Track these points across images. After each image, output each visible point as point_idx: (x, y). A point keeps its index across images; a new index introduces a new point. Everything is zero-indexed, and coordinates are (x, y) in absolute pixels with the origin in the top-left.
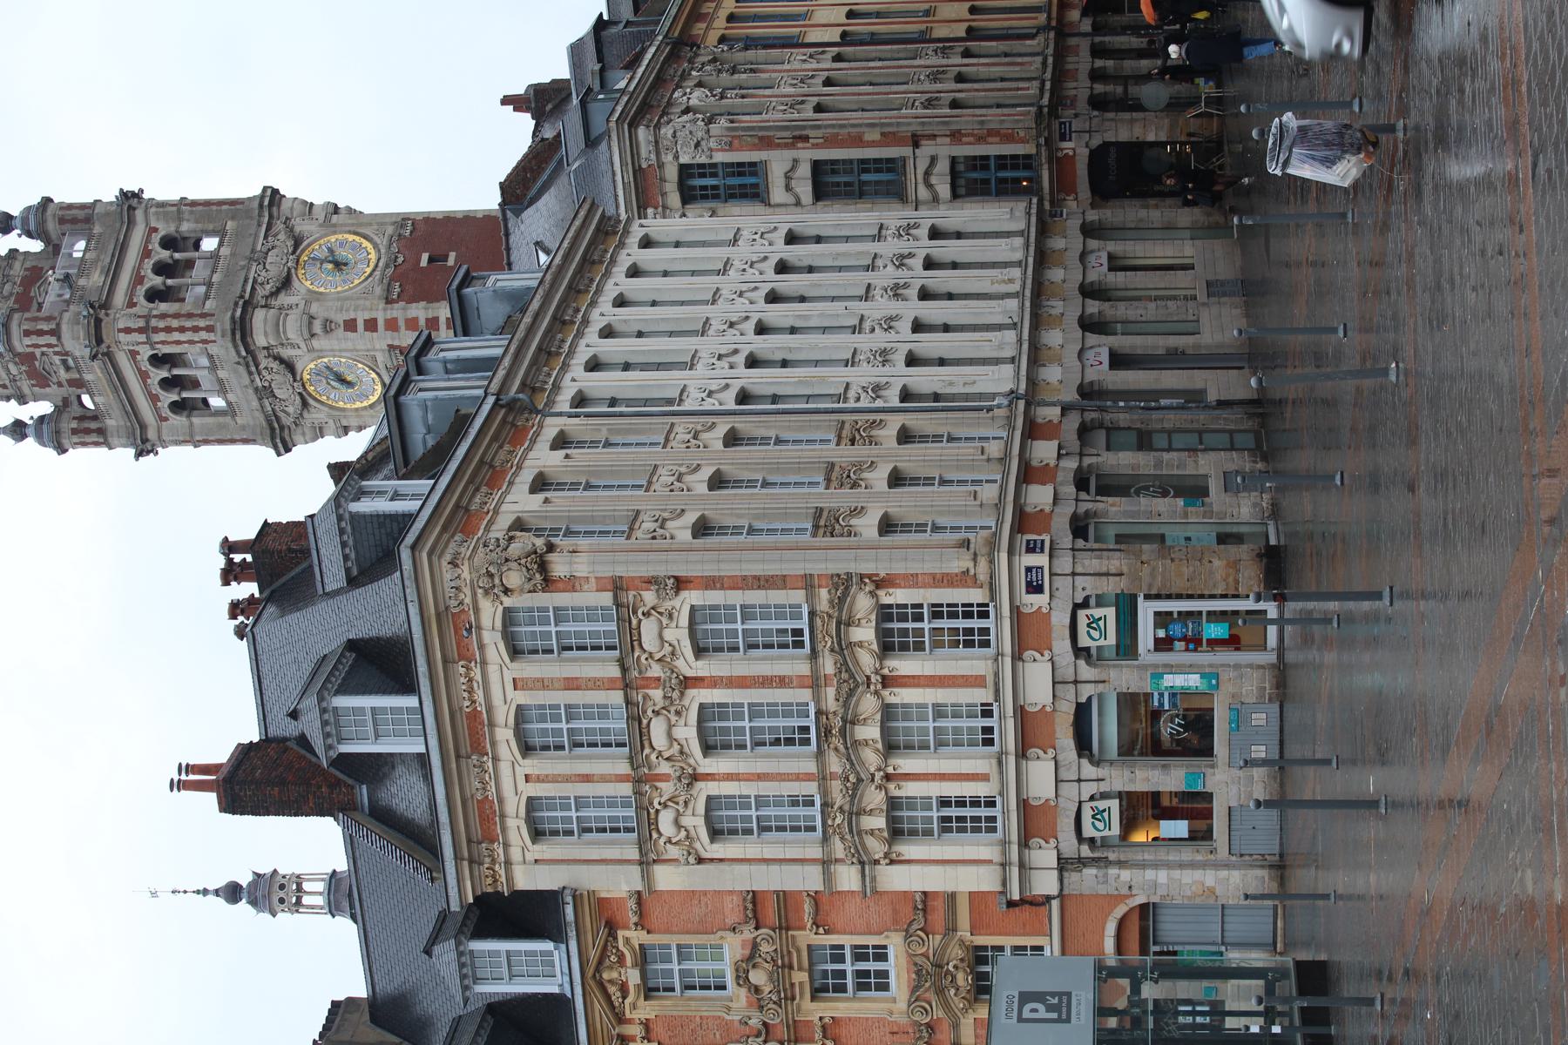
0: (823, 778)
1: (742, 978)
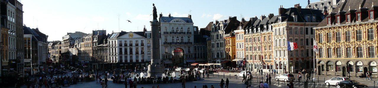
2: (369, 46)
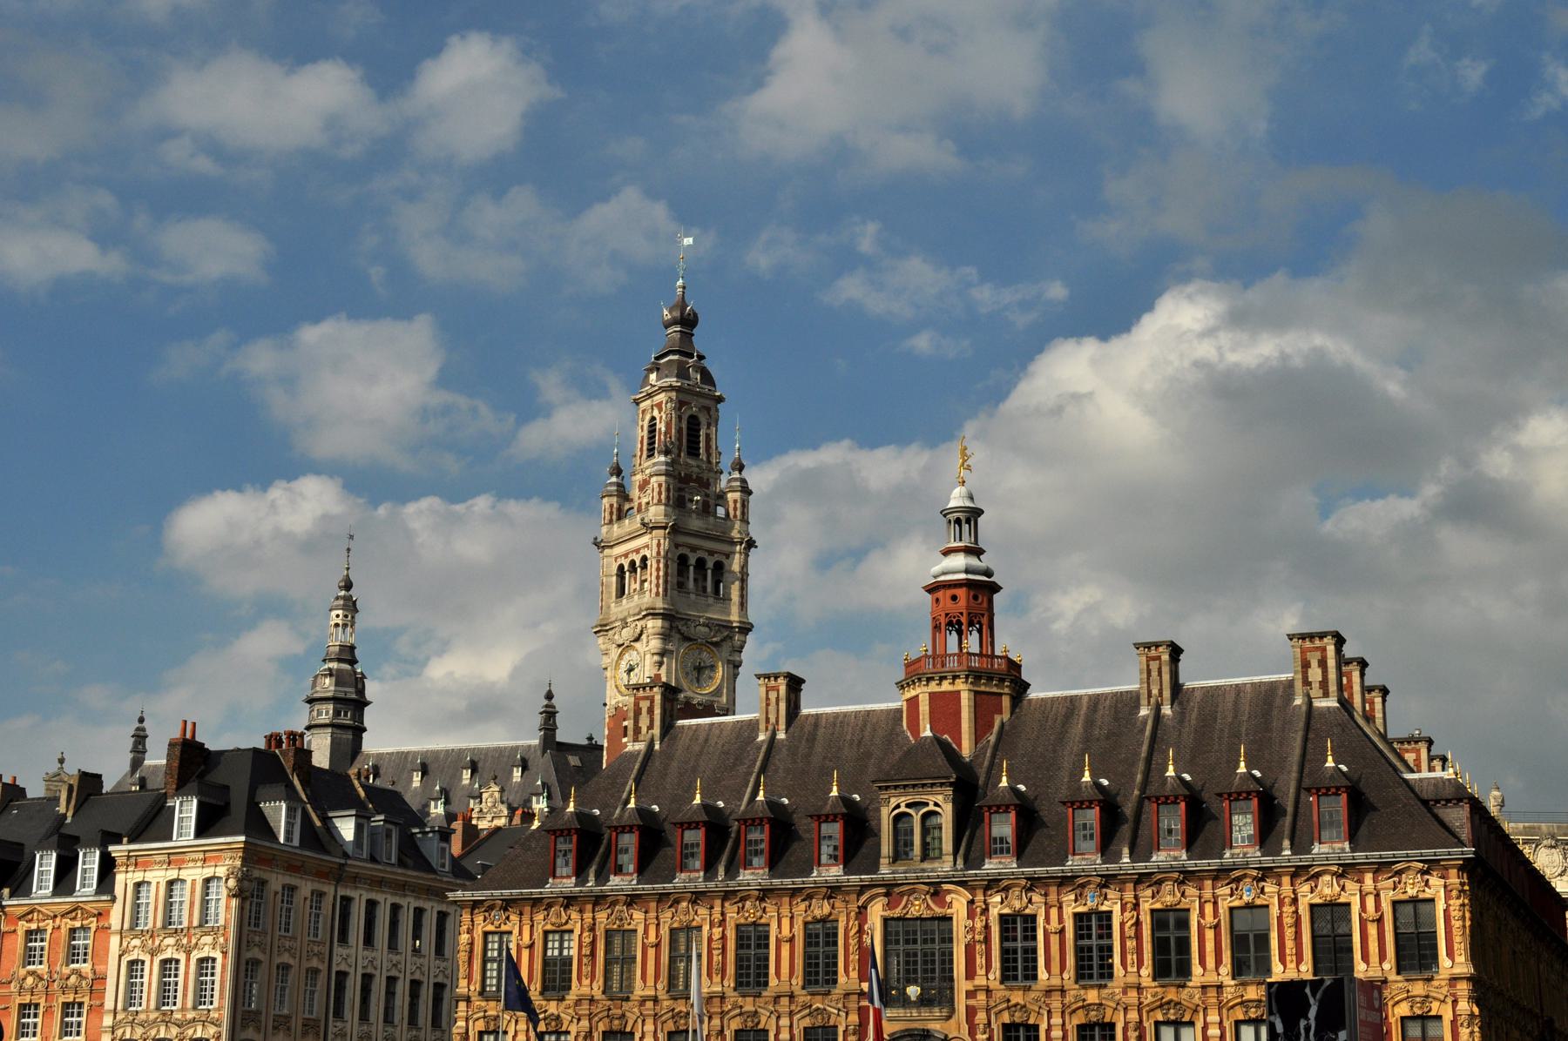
0: (147, 1011)
2: (807, 1022)
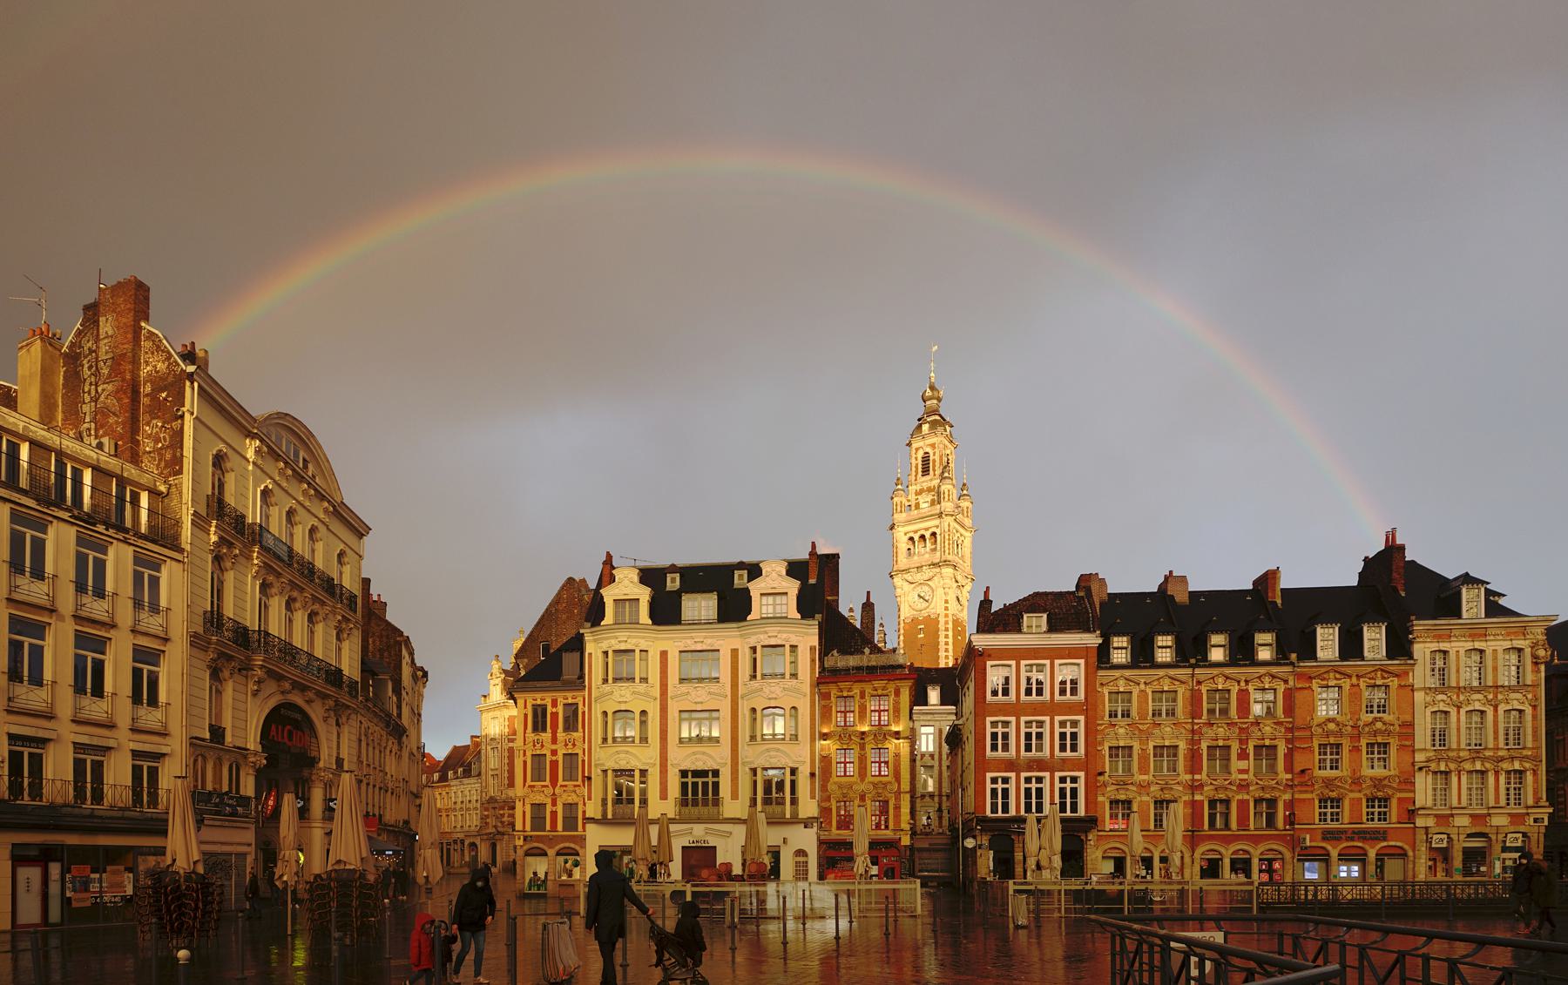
1: (1375, 719)
